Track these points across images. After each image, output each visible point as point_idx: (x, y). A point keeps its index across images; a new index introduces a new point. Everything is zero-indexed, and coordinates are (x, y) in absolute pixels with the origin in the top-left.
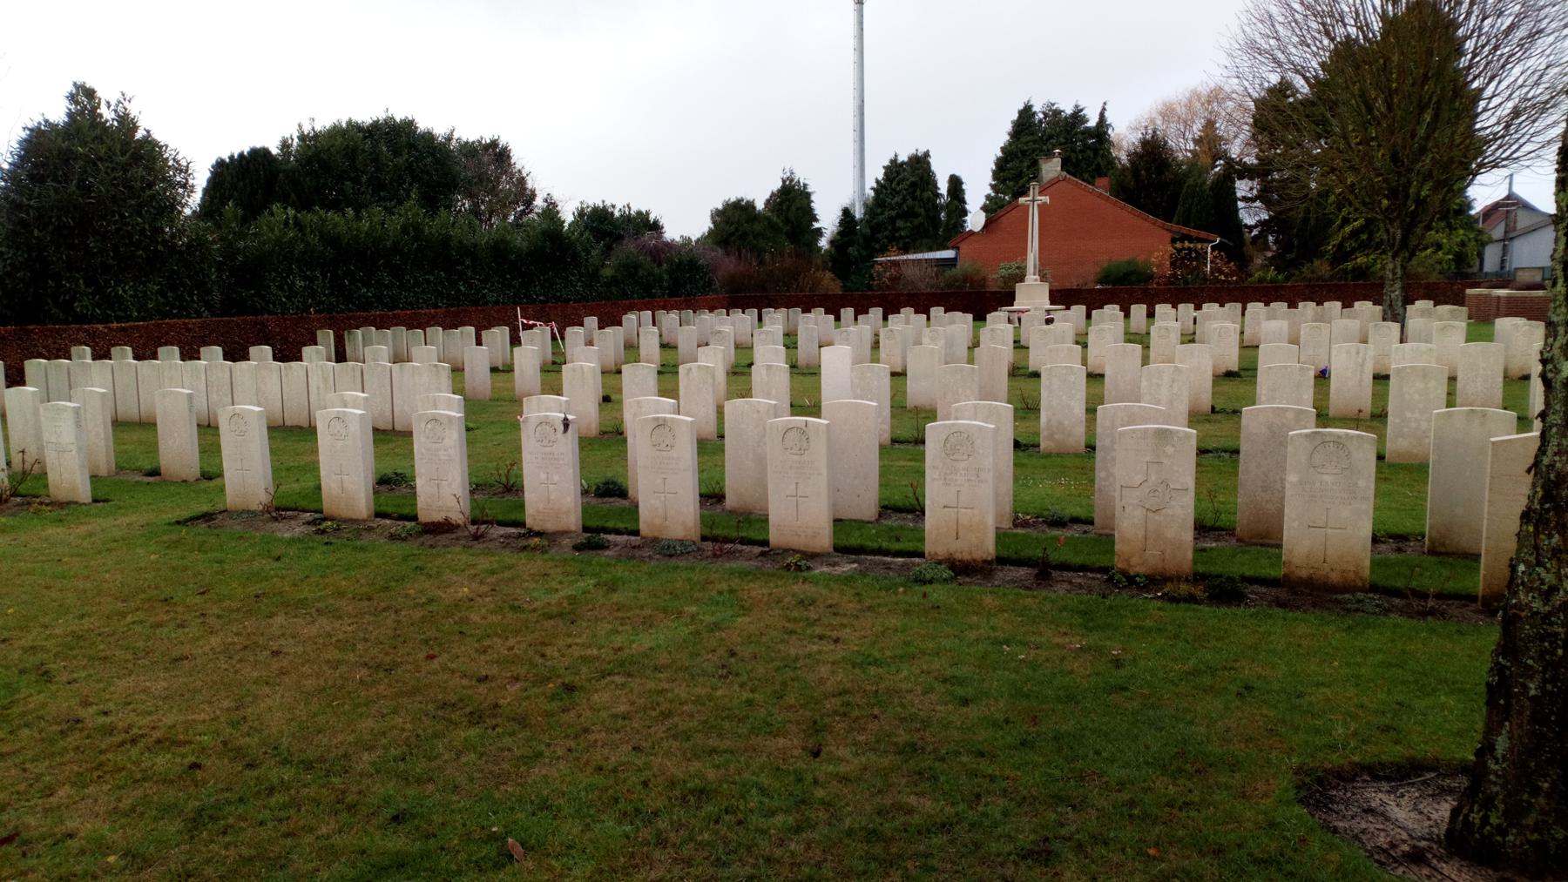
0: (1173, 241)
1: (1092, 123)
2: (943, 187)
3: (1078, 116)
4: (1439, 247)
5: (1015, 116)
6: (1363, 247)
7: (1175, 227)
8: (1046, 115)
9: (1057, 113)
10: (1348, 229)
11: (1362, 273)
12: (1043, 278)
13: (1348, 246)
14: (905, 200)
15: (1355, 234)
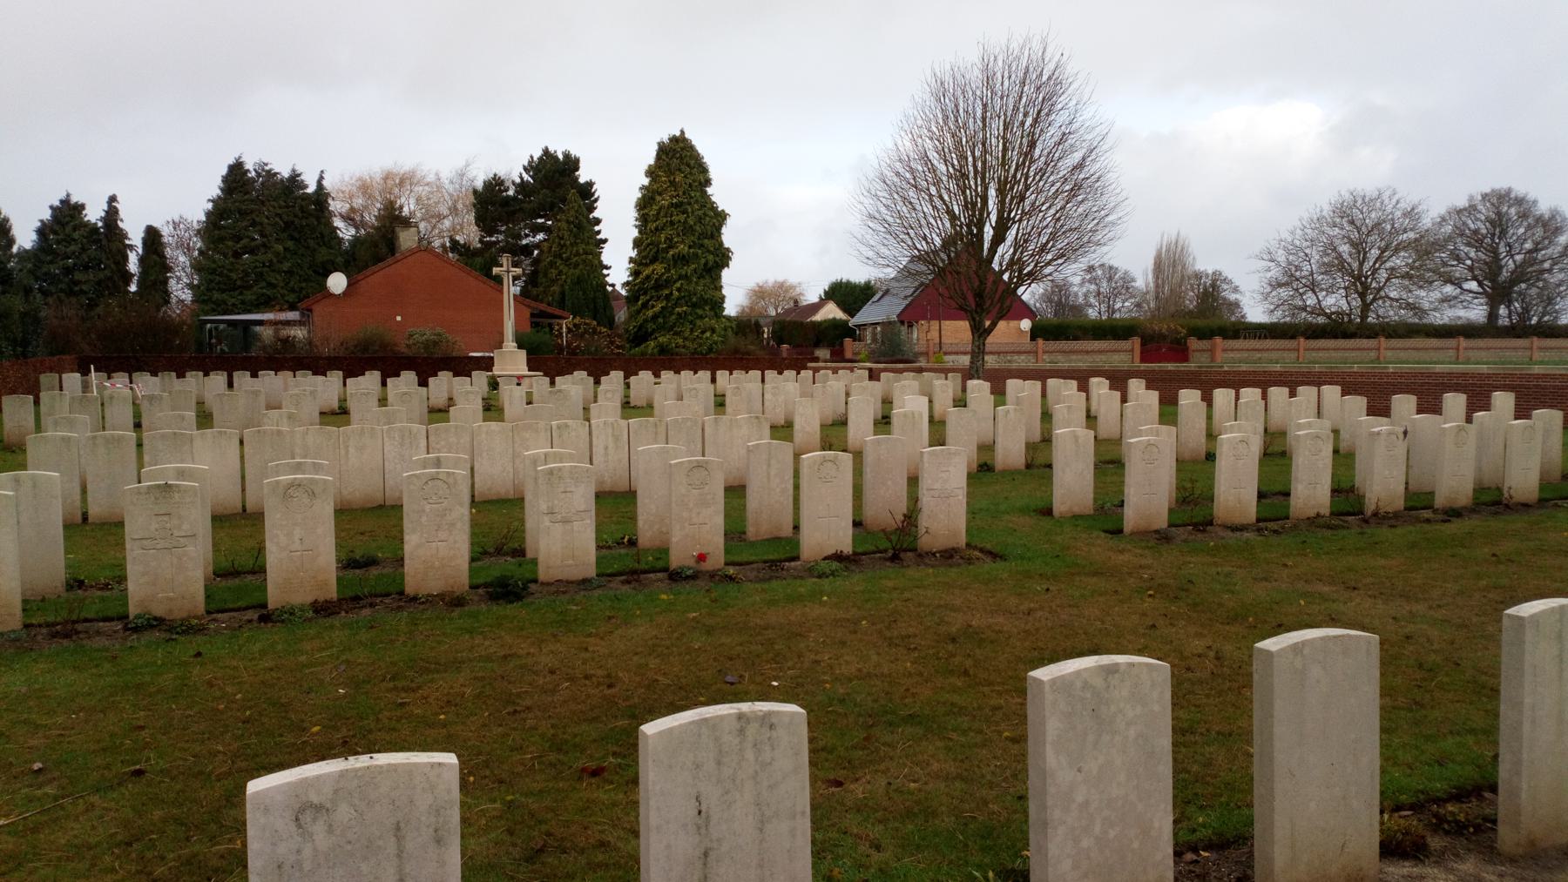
0: (532, 315)
1: (311, 189)
2: (136, 237)
3: (294, 181)
4: (713, 331)
5: (224, 171)
6: (661, 328)
7: (533, 304)
8: (259, 175)
9: (271, 175)
10: (650, 313)
11: (663, 350)
12: (520, 347)
13: (651, 327)
14: (83, 249)
15: (655, 317)
